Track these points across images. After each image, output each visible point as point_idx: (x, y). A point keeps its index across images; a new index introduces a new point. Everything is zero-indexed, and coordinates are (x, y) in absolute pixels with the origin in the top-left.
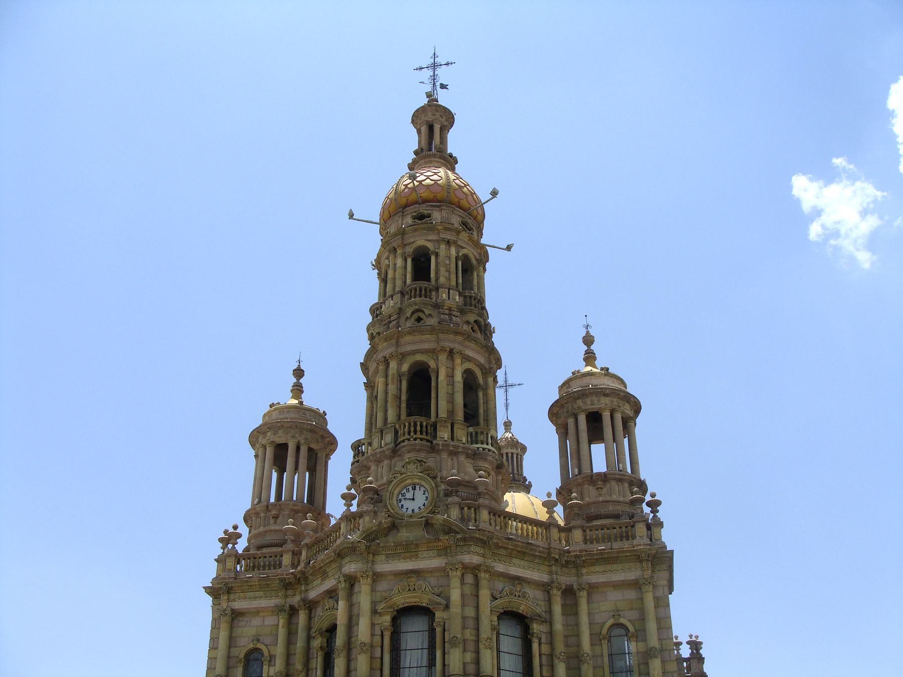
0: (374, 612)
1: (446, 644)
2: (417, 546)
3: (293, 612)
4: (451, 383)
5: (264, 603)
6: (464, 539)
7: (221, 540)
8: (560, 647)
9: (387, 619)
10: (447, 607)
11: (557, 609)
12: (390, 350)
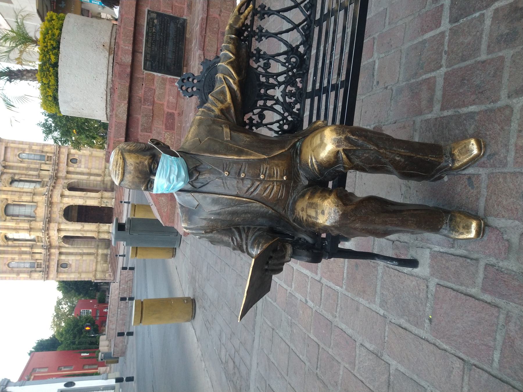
0: (5, 221)
8: (24, 172)
9: (8, 217)
10: (7, 199)
11: (11, 171)
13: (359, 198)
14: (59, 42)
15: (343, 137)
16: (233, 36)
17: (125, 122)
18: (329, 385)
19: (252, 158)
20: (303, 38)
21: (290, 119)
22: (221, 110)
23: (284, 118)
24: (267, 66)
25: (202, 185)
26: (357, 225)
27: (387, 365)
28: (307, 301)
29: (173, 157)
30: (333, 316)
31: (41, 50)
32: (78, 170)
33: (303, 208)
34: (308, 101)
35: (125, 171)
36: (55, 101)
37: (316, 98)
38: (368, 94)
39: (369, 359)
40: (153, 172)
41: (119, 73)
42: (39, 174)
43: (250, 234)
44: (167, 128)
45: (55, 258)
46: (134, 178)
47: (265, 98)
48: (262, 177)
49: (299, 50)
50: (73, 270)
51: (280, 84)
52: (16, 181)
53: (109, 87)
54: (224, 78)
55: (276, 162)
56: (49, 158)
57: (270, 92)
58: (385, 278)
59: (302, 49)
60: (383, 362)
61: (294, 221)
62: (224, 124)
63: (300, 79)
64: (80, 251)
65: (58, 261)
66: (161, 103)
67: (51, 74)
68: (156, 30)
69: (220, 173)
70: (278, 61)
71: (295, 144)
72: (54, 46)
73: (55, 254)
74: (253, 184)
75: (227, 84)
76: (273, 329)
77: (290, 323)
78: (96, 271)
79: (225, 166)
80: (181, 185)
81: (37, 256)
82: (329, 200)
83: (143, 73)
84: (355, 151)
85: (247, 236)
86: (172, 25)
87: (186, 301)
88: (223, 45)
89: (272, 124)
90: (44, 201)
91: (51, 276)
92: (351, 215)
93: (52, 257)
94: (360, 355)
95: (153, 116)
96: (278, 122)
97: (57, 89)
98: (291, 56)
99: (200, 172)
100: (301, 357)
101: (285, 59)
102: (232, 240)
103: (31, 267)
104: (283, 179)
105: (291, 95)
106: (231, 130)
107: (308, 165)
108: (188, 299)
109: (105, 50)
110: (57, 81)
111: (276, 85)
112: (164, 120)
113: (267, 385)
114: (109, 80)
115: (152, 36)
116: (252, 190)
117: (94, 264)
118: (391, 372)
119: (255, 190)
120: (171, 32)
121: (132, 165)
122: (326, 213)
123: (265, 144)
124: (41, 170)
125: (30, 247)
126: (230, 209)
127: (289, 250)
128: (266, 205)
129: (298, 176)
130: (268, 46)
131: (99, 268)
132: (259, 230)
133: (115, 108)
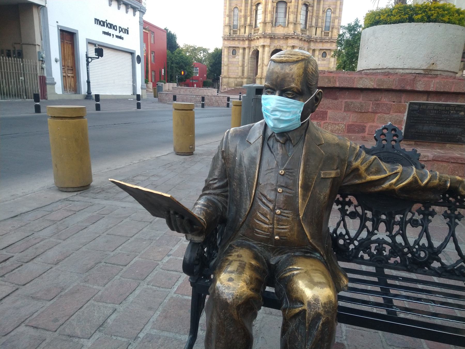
0: (273, 2)
8: (315, 14)
10: (291, 2)
13: (251, 325)
14: (435, 21)
15: (321, 311)
16: (449, 185)
17: (354, 87)
18: (87, 274)
19: (300, 202)
20: (450, 266)
21: (351, 247)
22: (357, 169)
23: (352, 240)
24: (414, 223)
25: (271, 147)
26: (215, 320)
27: (90, 336)
28: (169, 256)
29: (300, 114)
30: (149, 282)
31: (426, 6)
33: (241, 256)
34: (372, 269)
35: (284, 64)
36: (375, 22)
37: (376, 279)
38: (384, 340)
39: (100, 317)
40: (283, 93)
41: (405, 79)
42: (313, 27)
43: (220, 198)
44: (349, 126)
46: (277, 73)
47: (375, 219)
48: (278, 211)
49: (435, 262)
50: (230, 60)
51: (393, 237)
52: (307, 8)
53: (391, 71)
54: (396, 174)
55: (296, 228)
56: (327, 34)
57: (382, 226)
58: (175, 342)
59: (435, 264)
60: (92, 333)
61: (231, 246)
62: (341, 171)
63: (399, 262)
66: (376, 120)
67: (402, 16)
68: (453, 113)
69: (283, 165)
70: (420, 237)
71: (317, 251)
72: (431, 17)
73: (244, 44)
74: (270, 201)
75: (390, 176)
76: (151, 223)
77: (152, 238)
78: (229, 78)
79: (290, 171)
80: (271, 124)
81: (242, 30)
82: (245, 288)
83: (406, 102)
84: (304, 324)
85: (218, 195)
86: (460, 130)
87: (191, 147)
88: (438, 173)
89: (345, 226)
90: (289, 32)
92: (225, 313)
93: (241, 42)
94: (106, 307)
95: (362, 112)
96: (347, 233)
97: (386, 24)
98: (427, 252)
99: (284, 144)
100: (120, 248)
101: (423, 244)
102: (215, 179)
103: (234, 25)
104: (276, 235)
105: (380, 250)
106: (334, 179)
107: (290, 266)
108: (193, 149)
109: (429, 65)
110: (395, 22)
111: (391, 233)
112: (357, 123)
113: (104, 216)
114: (397, 70)
115: (446, 110)
116: (264, 200)
117: (235, 76)
118: (82, 340)
119: (264, 203)
120: (451, 129)
121: (291, 70)
122: (231, 283)
123: (318, 217)
124: (316, 28)
125: (251, 23)
126: (245, 176)
127: (198, 239)
128: (247, 215)
129: (279, 253)
130: (438, 226)
131: (231, 80)
132: (224, 207)
133: (369, 76)
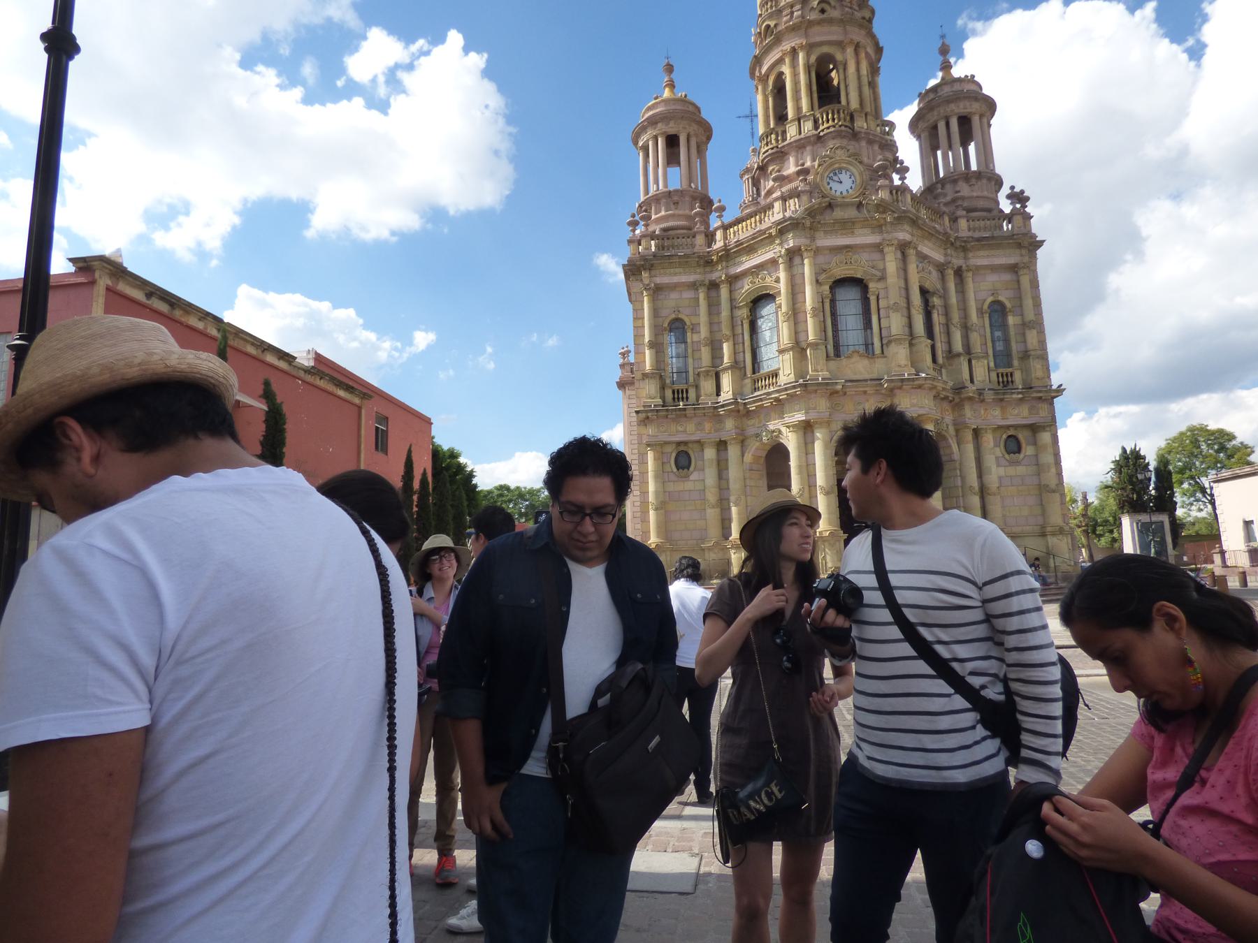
0: (817, 281)
1: (882, 312)
2: (853, 223)
3: (714, 286)
4: (859, 78)
5: (684, 278)
6: (898, 218)
7: (630, 224)
8: (956, 316)
9: (827, 288)
10: (883, 278)
11: (951, 285)
12: (798, 42)
32: (990, 461)
45: (707, 432)
64: (732, 498)
65: (698, 442)
91: (651, 430)
93: (707, 426)
124: (970, 361)
125: (736, 362)
